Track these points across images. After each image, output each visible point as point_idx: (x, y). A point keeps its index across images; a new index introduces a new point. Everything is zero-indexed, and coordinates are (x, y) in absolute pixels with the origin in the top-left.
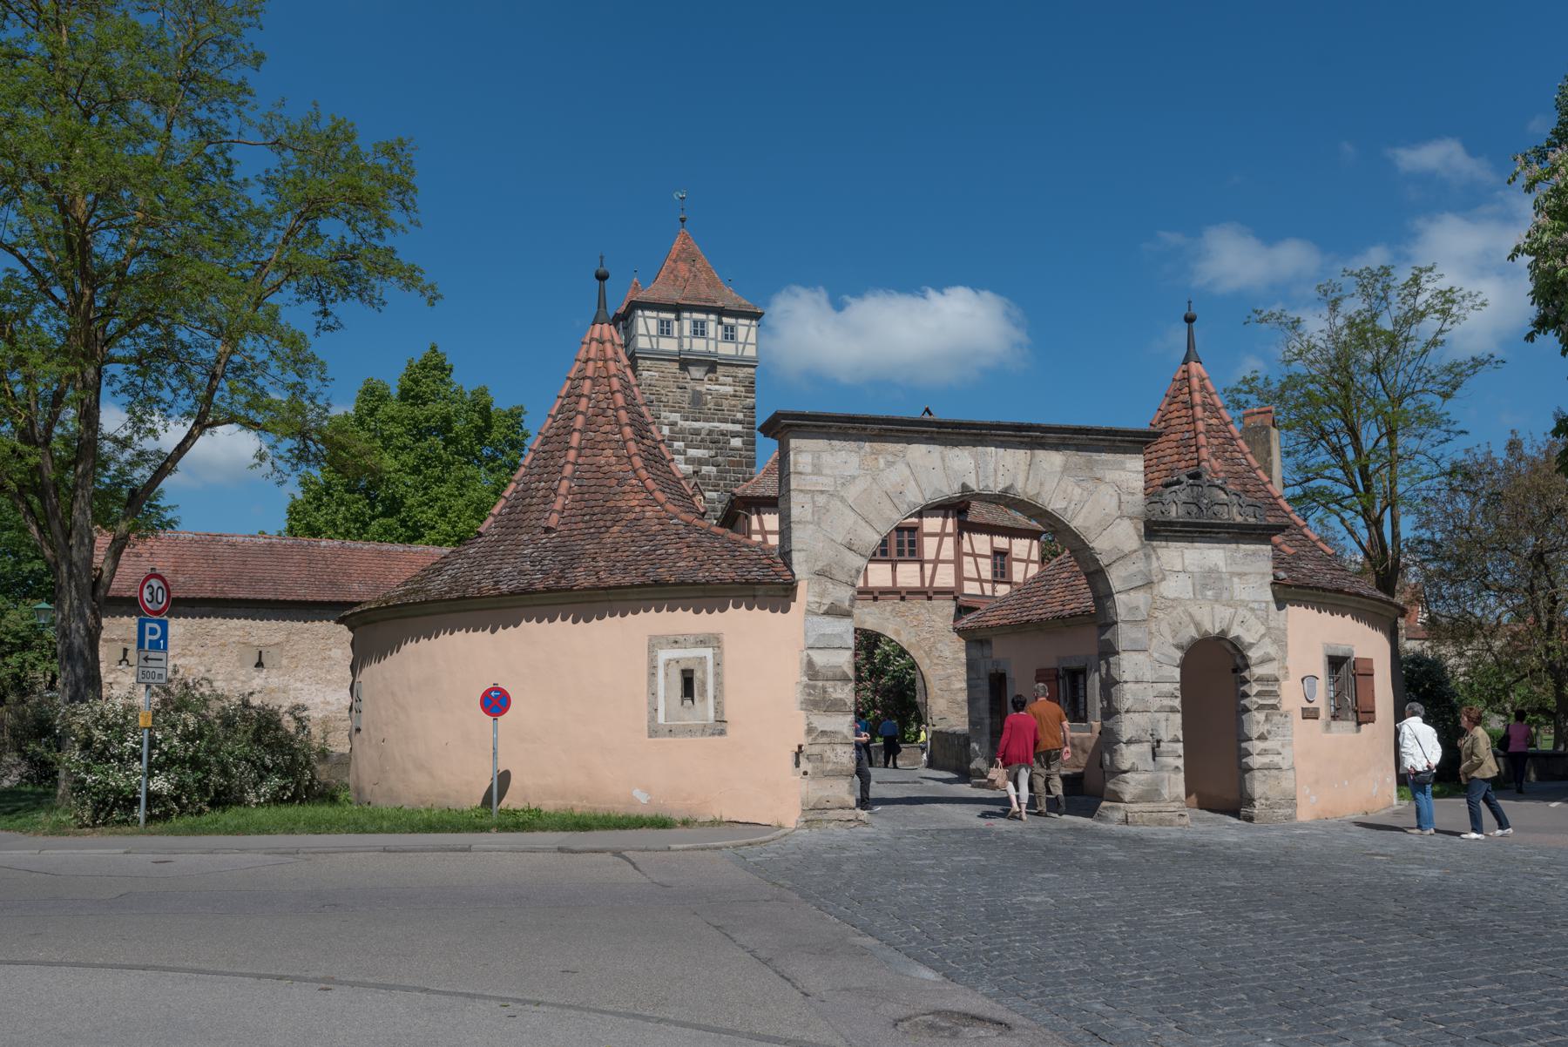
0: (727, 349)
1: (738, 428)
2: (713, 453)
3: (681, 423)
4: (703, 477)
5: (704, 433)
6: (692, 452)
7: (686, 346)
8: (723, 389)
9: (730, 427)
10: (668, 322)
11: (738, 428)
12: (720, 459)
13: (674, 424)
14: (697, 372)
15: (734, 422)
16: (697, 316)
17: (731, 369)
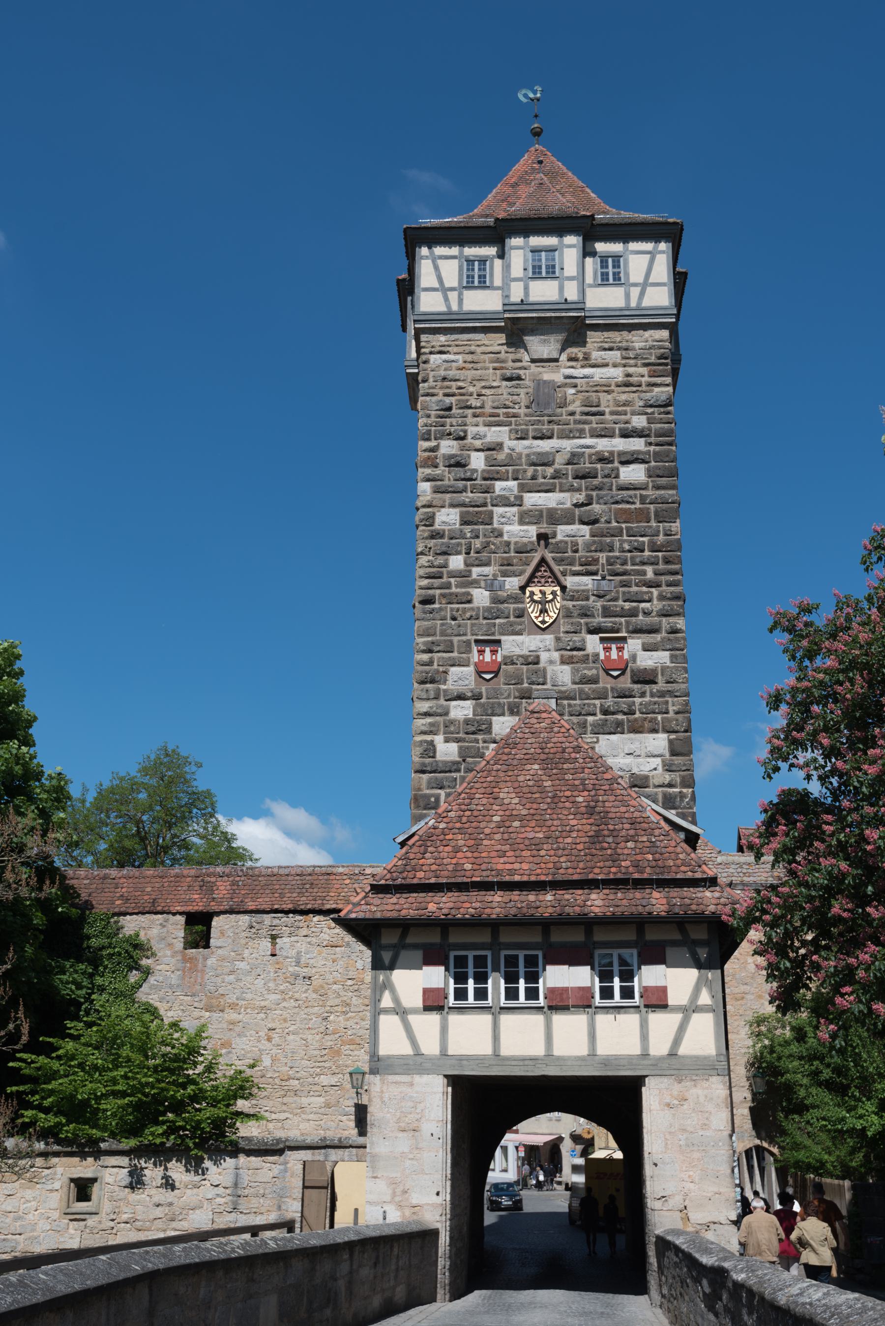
0: (603, 299)
1: (637, 444)
2: (581, 497)
3: (509, 443)
4: (560, 548)
5: (560, 459)
6: (532, 499)
7: (516, 294)
8: (598, 374)
9: (619, 444)
10: (483, 261)
11: (637, 444)
12: (596, 508)
13: (493, 448)
14: (542, 346)
15: (625, 435)
16: (536, 241)
17: (616, 336)
